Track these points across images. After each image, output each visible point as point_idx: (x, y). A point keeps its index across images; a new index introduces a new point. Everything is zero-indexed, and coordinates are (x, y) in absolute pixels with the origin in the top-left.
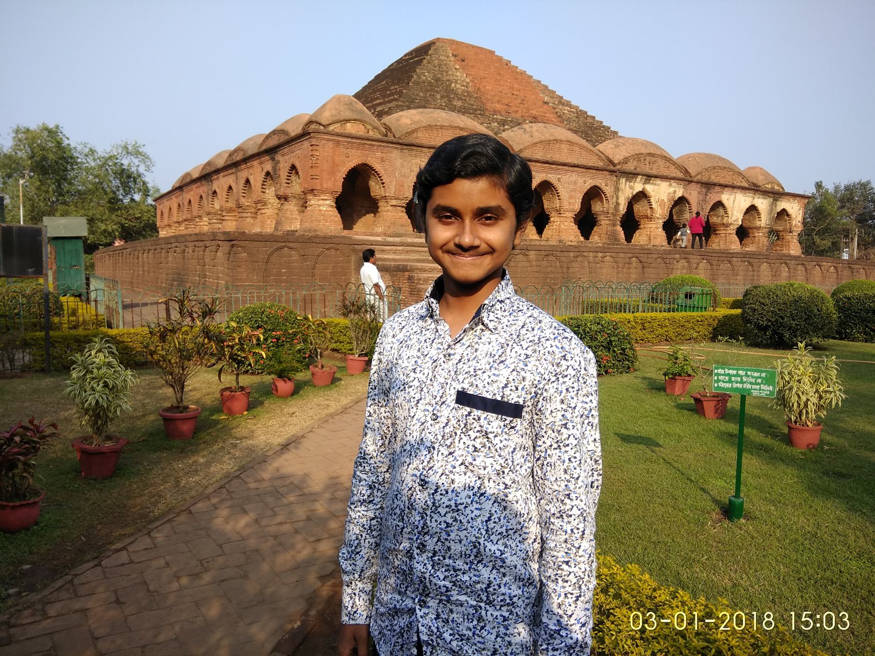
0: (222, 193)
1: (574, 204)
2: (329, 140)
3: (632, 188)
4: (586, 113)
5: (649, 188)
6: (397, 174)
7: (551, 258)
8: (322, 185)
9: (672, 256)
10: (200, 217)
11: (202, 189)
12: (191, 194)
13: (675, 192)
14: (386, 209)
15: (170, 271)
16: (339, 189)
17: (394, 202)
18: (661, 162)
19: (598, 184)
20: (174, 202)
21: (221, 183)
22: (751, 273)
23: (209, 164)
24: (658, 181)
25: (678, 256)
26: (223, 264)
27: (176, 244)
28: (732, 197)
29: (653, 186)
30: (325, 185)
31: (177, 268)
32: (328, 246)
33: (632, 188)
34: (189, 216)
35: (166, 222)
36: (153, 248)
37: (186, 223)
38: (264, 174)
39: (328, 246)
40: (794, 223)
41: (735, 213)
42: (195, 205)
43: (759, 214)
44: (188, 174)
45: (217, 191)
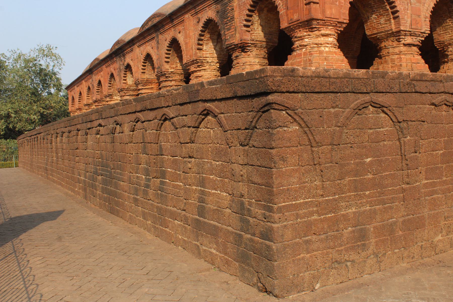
0: (137, 66)
8: (324, 12)
10: (110, 96)
11: (116, 66)
12: (102, 75)
14: (397, 50)
15: (91, 160)
16: (345, 17)
17: (409, 40)
20: (84, 86)
21: (135, 57)
23: (118, 42)
26: (218, 154)
27: (101, 121)
30: (328, 13)
31: (102, 157)
32: (438, 99)
34: (99, 97)
35: (77, 105)
36: (67, 129)
37: (96, 104)
38: (201, 24)
39: (438, 99)
42: (106, 86)
44: (96, 59)
45: (131, 64)
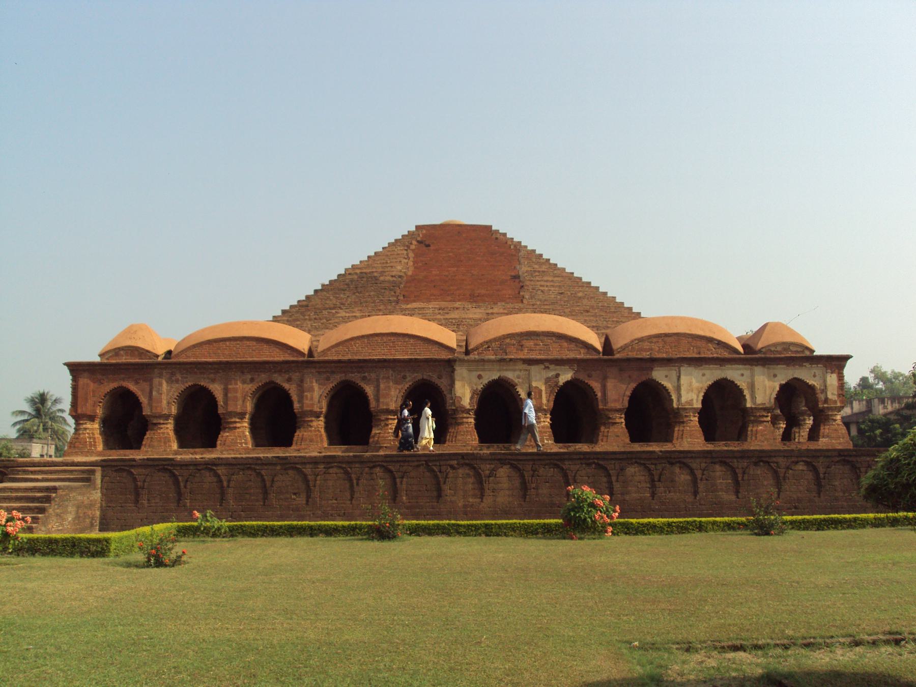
1: (388, 404)
2: (84, 371)
3: (480, 377)
4: (580, 279)
5: (510, 375)
6: (154, 393)
7: (250, 472)
9: (442, 463)
13: (557, 376)
18: (548, 341)
19: (425, 377)
22: (605, 479)
24: (525, 366)
25: (456, 462)
28: (674, 374)
29: (517, 373)
33: (480, 377)
40: (822, 397)
41: (683, 392)
43: (740, 391)
